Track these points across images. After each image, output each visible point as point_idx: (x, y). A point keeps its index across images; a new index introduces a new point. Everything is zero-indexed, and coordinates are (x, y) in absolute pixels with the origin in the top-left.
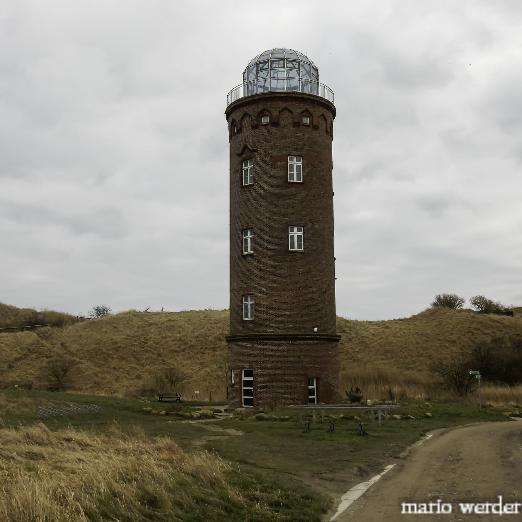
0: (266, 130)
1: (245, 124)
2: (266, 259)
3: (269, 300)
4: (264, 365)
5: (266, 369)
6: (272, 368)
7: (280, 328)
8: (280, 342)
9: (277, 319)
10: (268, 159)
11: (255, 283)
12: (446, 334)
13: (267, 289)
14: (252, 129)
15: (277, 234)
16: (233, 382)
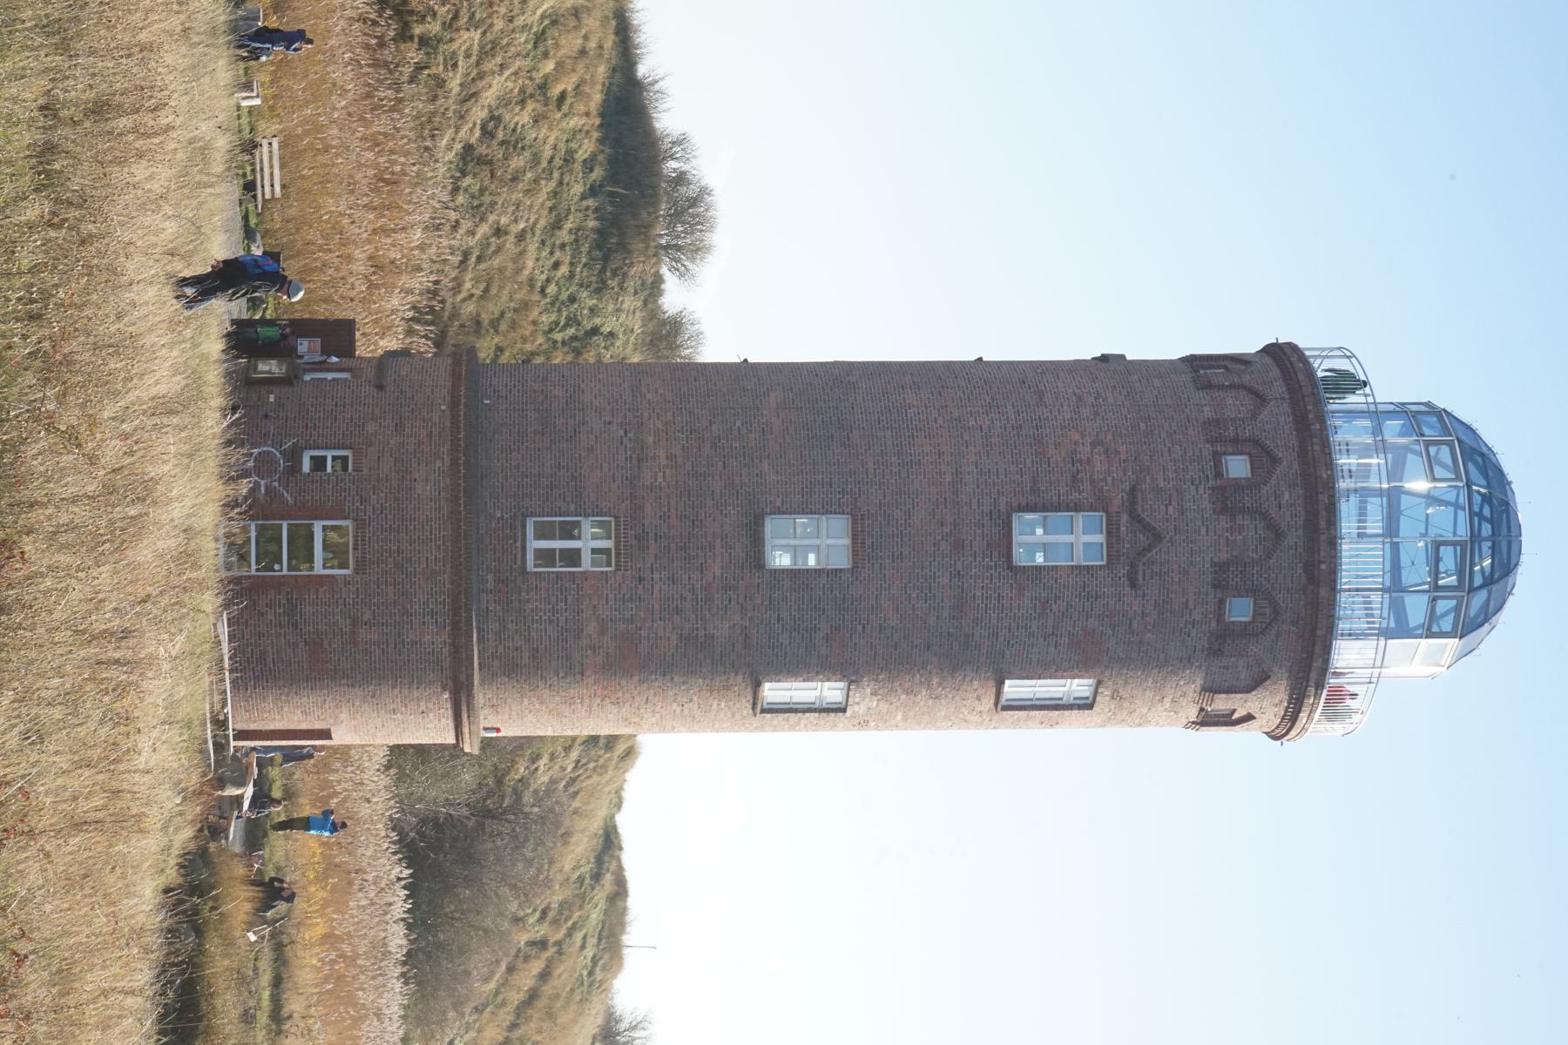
0: (1197, 616)
1: (1241, 529)
2: (737, 617)
3: (591, 628)
4: (367, 616)
5: (354, 624)
6: (355, 643)
7: (496, 663)
8: (446, 665)
9: (526, 654)
10: (1093, 623)
11: (656, 576)
12: (531, 328)
13: (632, 620)
14: (1214, 564)
15: (824, 651)
16: (307, 378)
